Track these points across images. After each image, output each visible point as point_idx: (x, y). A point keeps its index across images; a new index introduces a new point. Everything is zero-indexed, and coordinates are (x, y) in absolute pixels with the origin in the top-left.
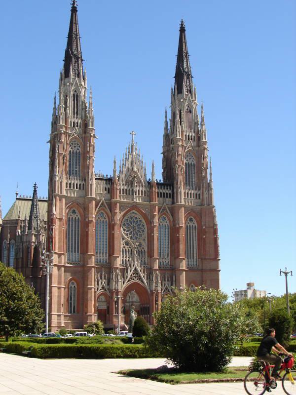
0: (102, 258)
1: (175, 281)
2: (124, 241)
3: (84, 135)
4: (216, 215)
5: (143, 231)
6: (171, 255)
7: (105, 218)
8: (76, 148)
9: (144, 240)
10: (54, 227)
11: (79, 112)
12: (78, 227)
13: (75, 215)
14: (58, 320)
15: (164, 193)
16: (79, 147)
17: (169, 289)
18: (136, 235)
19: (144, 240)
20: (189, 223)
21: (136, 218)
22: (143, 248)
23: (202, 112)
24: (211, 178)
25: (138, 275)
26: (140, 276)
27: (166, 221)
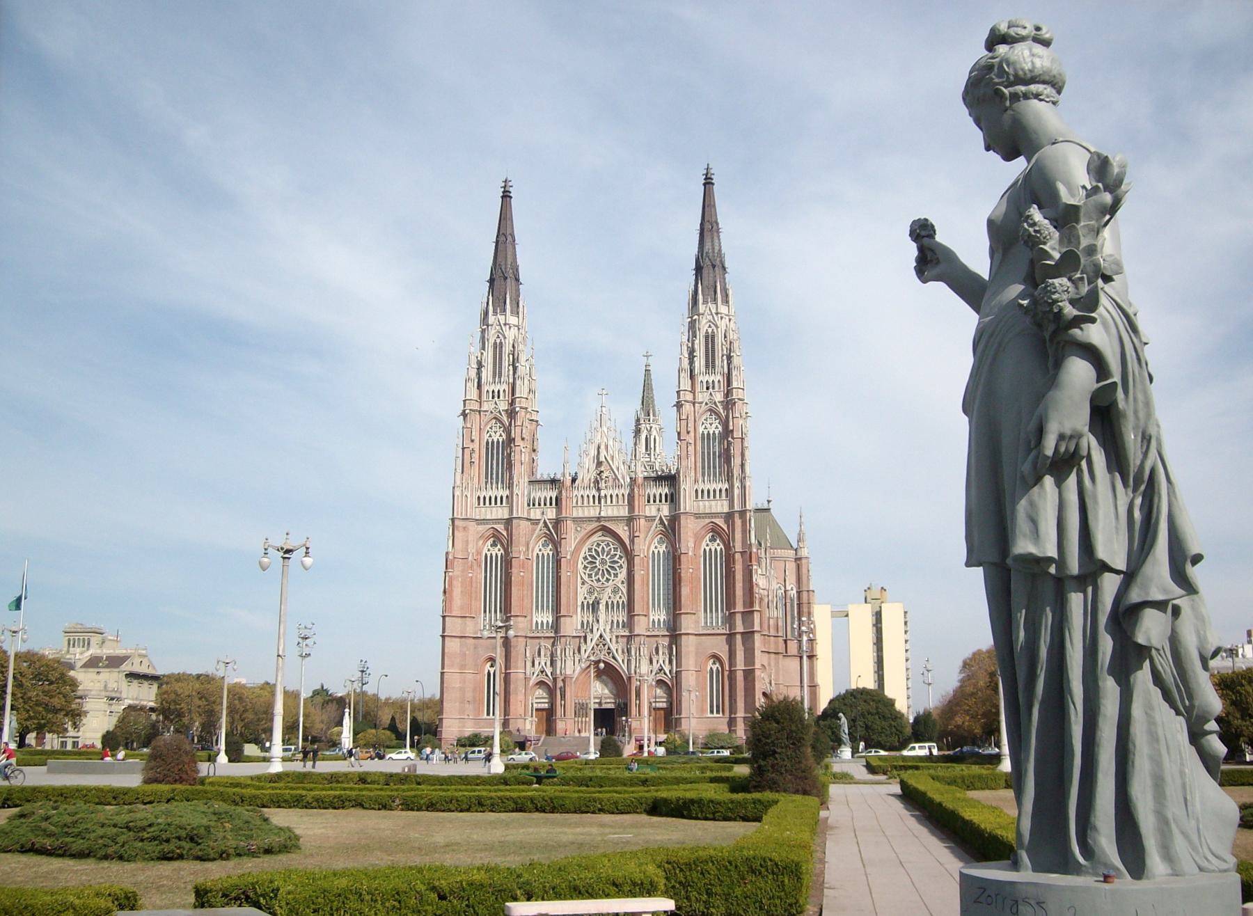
8: (498, 434)
9: (623, 582)
10: (450, 574)
14: (459, 727)
17: (667, 669)
18: (607, 575)
20: (707, 545)
21: (608, 545)
25: (606, 647)
26: (609, 649)
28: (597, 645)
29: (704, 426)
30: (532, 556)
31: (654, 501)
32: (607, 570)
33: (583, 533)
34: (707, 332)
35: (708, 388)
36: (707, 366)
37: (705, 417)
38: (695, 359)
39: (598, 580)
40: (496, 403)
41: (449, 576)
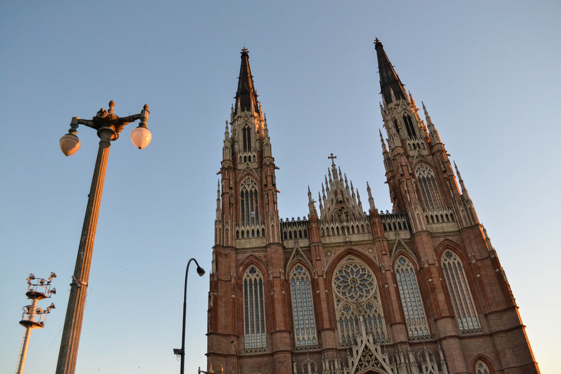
0: (306, 339)
1: (445, 360)
2: (341, 304)
3: (259, 169)
4: (489, 236)
5: (371, 284)
6: (428, 317)
7: (304, 274)
8: (251, 186)
11: (253, 145)
12: (261, 292)
13: (255, 274)
15: (394, 224)
16: (255, 184)
19: (375, 298)
20: (446, 260)
21: (356, 266)
22: (376, 311)
23: (426, 113)
24: (463, 186)
25: (373, 357)
26: (376, 359)
27: (407, 262)
28: (364, 356)
29: (418, 173)
30: (289, 278)
31: (390, 229)
32: (358, 286)
33: (333, 256)
34: (404, 116)
35: (415, 148)
36: (410, 134)
37: (417, 167)
38: (400, 130)
39: (352, 297)
40: (248, 164)
41: (214, 295)
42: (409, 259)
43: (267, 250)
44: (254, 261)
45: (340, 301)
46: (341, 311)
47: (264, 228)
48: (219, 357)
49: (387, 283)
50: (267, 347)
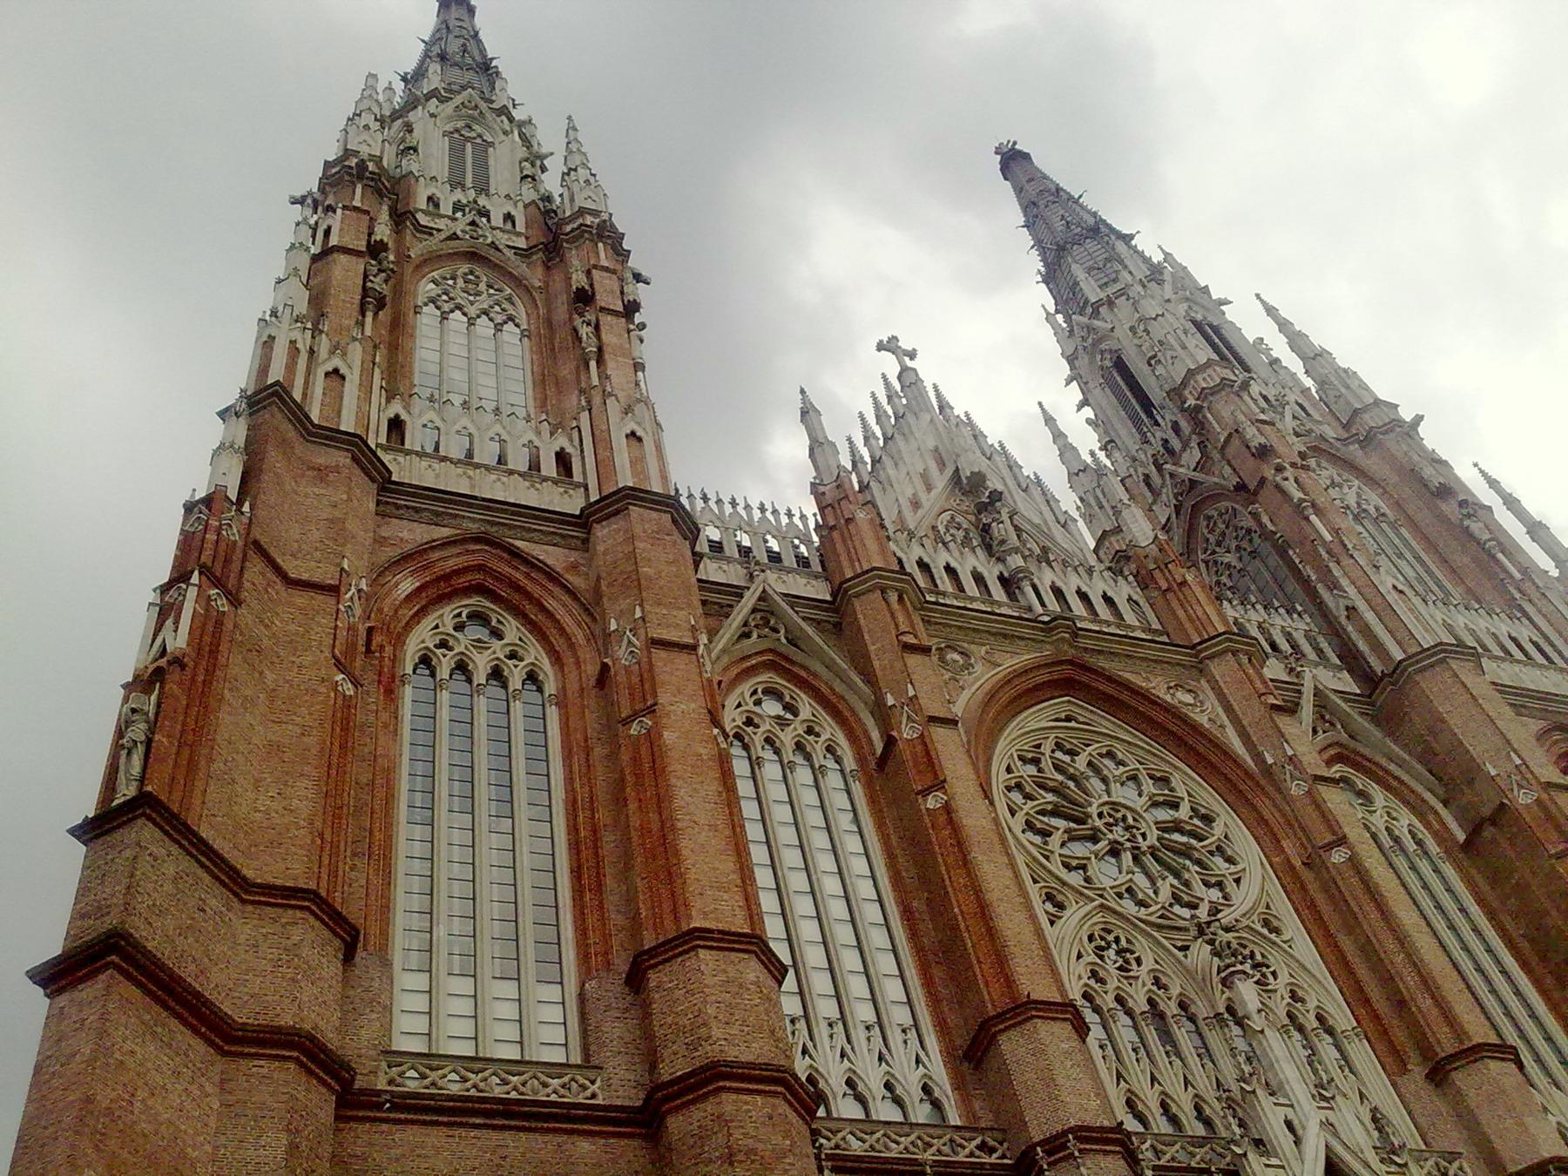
2: (1074, 913)
42: (1388, 788)
43: (586, 541)
44: (499, 577)
45: (1061, 906)
46: (1079, 956)
47: (569, 450)
48: (174, 1023)
49: (1342, 841)
50: (588, 1064)
